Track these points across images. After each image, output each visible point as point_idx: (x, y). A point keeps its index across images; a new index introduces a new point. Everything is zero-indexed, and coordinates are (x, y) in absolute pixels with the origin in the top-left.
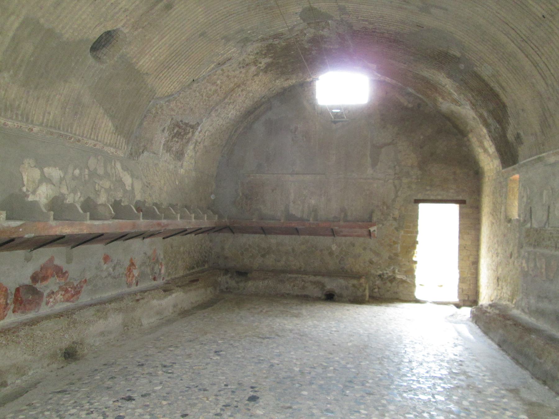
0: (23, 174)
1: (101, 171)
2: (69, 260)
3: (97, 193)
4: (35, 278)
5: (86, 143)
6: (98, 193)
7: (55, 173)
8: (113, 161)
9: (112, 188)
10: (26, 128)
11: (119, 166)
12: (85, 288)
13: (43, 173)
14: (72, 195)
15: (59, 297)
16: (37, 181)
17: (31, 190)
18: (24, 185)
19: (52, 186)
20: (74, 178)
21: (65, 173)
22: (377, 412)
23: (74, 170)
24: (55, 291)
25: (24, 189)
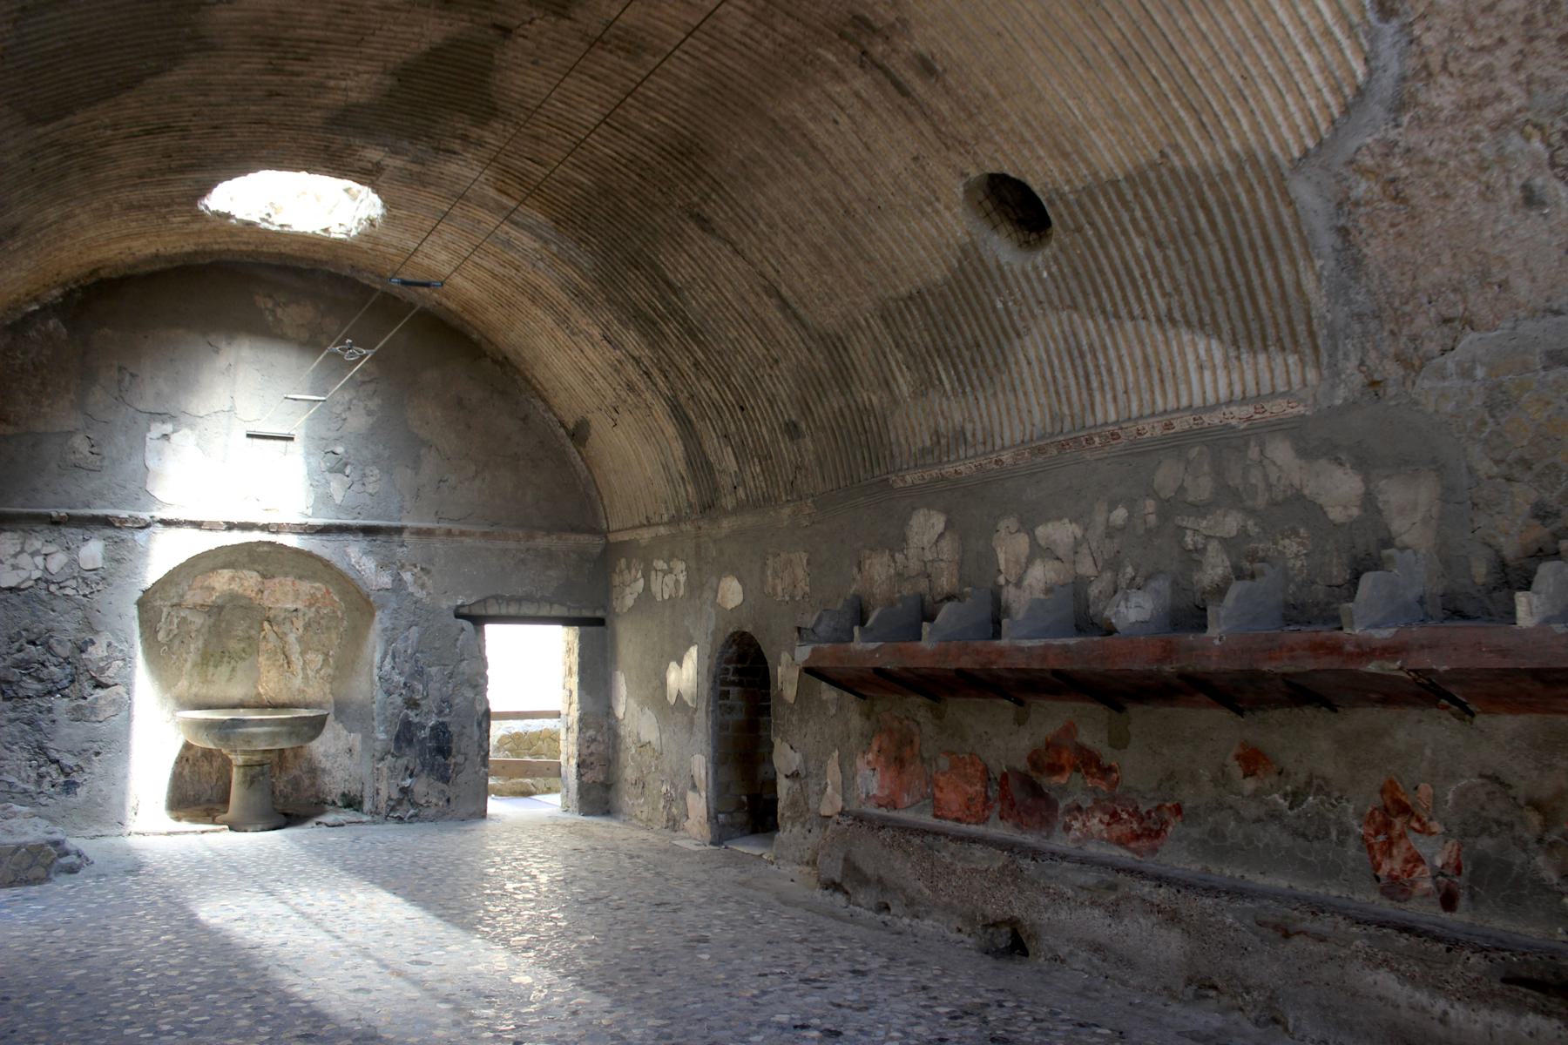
0: (999, 550)
1: (1202, 488)
2: (1119, 741)
3: (1193, 558)
5: (1140, 434)
6: (1195, 556)
7: (1060, 532)
8: (1252, 444)
9: (1253, 529)
11: (1281, 452)
12: (1174, 827)
13: (1033, 540)
14: (1108, 575)
15: (1095, 823)
16: (1023, 560)
17: (1013, 579)
18: (999, 571)
19: (1057, 564)
20: (1111, 532)
21: (1086, 529)
22: (270, 1010)
23: (1110, 511)
24: (1084, 806)
25: (1001, 580)
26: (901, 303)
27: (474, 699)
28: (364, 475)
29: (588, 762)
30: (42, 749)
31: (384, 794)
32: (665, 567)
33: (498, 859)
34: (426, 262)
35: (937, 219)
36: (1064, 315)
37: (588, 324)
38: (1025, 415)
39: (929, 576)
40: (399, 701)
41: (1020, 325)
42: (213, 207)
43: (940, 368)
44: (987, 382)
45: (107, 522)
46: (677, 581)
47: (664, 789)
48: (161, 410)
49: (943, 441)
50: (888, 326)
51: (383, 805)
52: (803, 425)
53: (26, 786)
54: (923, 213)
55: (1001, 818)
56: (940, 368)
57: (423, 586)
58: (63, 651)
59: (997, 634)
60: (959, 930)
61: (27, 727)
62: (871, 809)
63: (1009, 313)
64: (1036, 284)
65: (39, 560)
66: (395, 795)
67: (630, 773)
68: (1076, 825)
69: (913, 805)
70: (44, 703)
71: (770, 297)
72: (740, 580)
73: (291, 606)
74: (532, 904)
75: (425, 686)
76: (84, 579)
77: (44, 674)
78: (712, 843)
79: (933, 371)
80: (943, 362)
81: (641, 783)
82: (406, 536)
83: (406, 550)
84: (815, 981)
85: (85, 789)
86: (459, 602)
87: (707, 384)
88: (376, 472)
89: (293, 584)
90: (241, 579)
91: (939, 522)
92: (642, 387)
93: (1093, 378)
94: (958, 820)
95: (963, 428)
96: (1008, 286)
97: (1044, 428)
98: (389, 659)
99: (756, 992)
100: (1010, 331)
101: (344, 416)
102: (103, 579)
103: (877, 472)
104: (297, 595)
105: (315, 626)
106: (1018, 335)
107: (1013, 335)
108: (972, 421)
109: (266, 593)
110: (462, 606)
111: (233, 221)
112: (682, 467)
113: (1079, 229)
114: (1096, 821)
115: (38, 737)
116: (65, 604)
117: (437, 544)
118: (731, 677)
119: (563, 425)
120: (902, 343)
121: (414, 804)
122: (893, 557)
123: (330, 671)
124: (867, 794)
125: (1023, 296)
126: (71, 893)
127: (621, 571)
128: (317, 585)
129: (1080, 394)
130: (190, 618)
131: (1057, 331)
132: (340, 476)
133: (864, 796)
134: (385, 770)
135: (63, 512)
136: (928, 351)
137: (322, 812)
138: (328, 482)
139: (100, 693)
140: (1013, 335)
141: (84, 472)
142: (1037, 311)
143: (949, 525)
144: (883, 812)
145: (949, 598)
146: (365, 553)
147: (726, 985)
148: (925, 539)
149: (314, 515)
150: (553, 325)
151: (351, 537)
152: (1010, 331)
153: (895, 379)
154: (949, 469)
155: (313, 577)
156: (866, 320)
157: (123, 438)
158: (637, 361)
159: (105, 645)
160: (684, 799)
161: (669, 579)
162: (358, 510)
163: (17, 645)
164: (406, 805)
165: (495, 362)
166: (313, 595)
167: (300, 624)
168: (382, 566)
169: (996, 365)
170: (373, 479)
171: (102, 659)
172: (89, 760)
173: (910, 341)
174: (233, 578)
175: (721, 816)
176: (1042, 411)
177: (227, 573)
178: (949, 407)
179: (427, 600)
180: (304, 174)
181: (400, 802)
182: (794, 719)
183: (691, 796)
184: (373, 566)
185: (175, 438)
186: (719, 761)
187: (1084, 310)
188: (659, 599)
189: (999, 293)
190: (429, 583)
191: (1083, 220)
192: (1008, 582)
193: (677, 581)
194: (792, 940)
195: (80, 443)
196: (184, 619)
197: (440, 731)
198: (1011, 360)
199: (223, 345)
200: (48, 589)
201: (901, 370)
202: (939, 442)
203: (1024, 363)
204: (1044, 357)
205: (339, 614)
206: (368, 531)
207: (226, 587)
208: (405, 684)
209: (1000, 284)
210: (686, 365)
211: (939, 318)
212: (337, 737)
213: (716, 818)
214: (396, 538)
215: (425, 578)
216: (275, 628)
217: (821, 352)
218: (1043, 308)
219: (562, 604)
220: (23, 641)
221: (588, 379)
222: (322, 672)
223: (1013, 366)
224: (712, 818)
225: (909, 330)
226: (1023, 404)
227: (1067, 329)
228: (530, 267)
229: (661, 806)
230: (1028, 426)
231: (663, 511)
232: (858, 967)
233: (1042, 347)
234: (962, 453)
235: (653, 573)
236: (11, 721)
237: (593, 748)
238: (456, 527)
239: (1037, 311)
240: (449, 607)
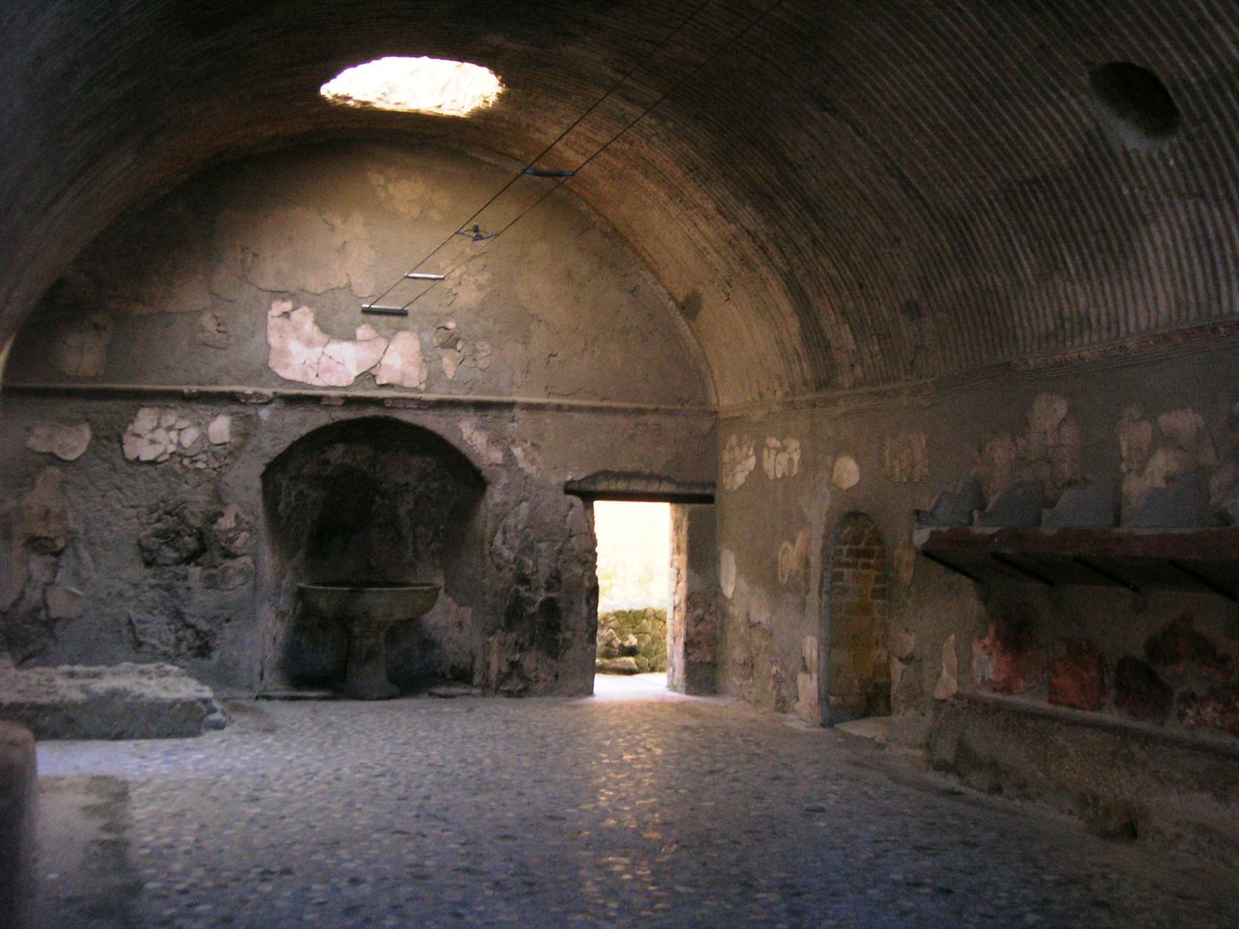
4: (1153, 649)
7: (1184, 422)
10: (1114, 348)
15: (1209, 712)
16: (1145, 447)
17: (1134, 467)
22: (431, 848)
24: (1199, 694)
25: (1123, 467)
26: (1027, 188)
27: (583, 575)
28: (475, 351)
29: (695, 641)
30: (178, 615)
31: (494, 667)
32: (778, 444)
33: (612, 733)
34: (537, 136)
35: (1063, 106)
36: (1190, 203)
37: (702, 199)
38: (1150, 301)
39: (1050, 462)
40: (509, 575)
41: (1146, 211)
42: (334, 92)
43: (1066, 253)
44: (1112, 267)
45: (233, 398)
46: (791, 460)
47: (774, 670)
48: (281, 288)
49: (1068, 326)
50: (1012, 209)
51: (493, 677)
52: (924, 304)
53: (166, 649)
54: (1049, 99)
55: (1117, 704)
56: (1066, 253)
57: (533, 462)
58: (196, 522)
59: (1117, 522)
60: (1071, 813)
61: (165, 593)
62: (986, 694)
63: (1136, 202)
64: (1163, 172)
65: (173, 435)
66: (505, 669)
67: (738, 654)
68: (1190, 712)
69: (1028, 689)
70: (180, 570)
71: (892, 175)
72: (857, 461)
74: (651, 774)
75: (535, 562)
76: (214, 453)
77: (179, 544)
78: (823, 725)
79: (1058, 254)
80: (1069, 247)
81: (749, 666)
82: (517, 412)
83: (517, 425)
84: (928, 848)
86: (569, 478)
87: (826, 262)
88: (487, 347)
91: (1061, 408)
92: (758, 262)
93: (1219, 266)
94: (1073, 706)
95: (1087, 312)
96: (1135, 174)
97: (1170, 317)
99: (872, 855)
100: (1137, 217)
101: (455, 291)
103: (1000, 355)
106: (1145, 222)
107: (1139, 222)
108: (1096, 305)
109: (378, 468)
110: (572, 482)
111: (351, 103)
112: (797, 342)
113: (1206, 118)
114: (1210, 710)
115: (176, 602)
117: (547, 419)
118: (844, 559)
119: (673, 298)
120: (1027, 226)
121: (523, 678)
122: (1014, 440)
124: (983, 679)
125: (1151, 183)
126: (223, 745)
127: (732, 448)
128: (427, 459)
129: (1206, 283)
131: (1183, 218)
132: (452, 351)
133: (979, 680)
134: (496, 644)
135: (195, 389)
136: (1053, 235)
137: (435, 685)
138: (440, 358)
139: (228, 563)
140: (1139, 222)
141: (212, 350)
142: (1164, 198)
143: (1072, 411)
144: (999, 696)
145: (1069, 484)
146: (481, 428)
147: (843, 848)
148: (1048, 424)
149: (427, 391)
150: (666, 198)
151: (463, 413)
152: (1137, 217)
153: (1020, 262)
154: (1073, 354)
156: (991, 203)
157: (246, 316)
158: (753, 236)
160: (794, 680)
161: (783, 458)
162: (469, 385)
163: (155, 516)
164: (515, 679)
165: (605, 234)
167: (410, 498)
168: (494, 441)
169: (1122, 251)
170: (483, 354)
171: (231, 530)
172: (220, 626)
173: (1034, 223)
174: (346, 453)
175: (832, 699)
176: (1167, 298)
177: (340, 448)
178: (1074, 290)
179: (537, 476)
180: (425, 59)
181: (508, 676)
182: (910, 602)
183: (802, 678)
184: (484, 441)
185: (295, 315)
186: (831, 643)
187: (1211, 198)
188: (771, 477)
189: (1125, 179)
190: (539, 458)
191: (1210, 111)
192: (1130, 470)
193: (791, 460)
194: (905, 814)
195: (207, 321)
197: (550, 607)
198: (1137, 245)
199: (337, 222)
200: (181, 462)
201: (1025, 252)
202: (1063, 325)
203: (1149, 250)
204: (1170, 243)
206: (481, 406)
207: (339, 461)
208: (515, 559)
209: (1127, 171)
210: (803, 240)
211: (1065, 203)
213: (827, 700)
214: (507, 414)
215: (536, 454)
217: (943, 231)
218: (1169, 196)
219: (669, 480)
220: (160, 512)
221: (701, 253)
222: (432, 546)
223: (1139, 252)
224: (823, 699)
225: (1035, 213)
226: (1149, 292)
227: (1194, 216)
228: (644, 141)
229: (770, 688)
230: (1153, 312)
231: (776, 386)
232: (967, 839)
233: (1168, 235)
234: (1086, 339)
235: (765, 452)
236: (152, 587)
237: (700, 627)
238: (566, 401)
239: (1164, 198)
240: (559, 484)
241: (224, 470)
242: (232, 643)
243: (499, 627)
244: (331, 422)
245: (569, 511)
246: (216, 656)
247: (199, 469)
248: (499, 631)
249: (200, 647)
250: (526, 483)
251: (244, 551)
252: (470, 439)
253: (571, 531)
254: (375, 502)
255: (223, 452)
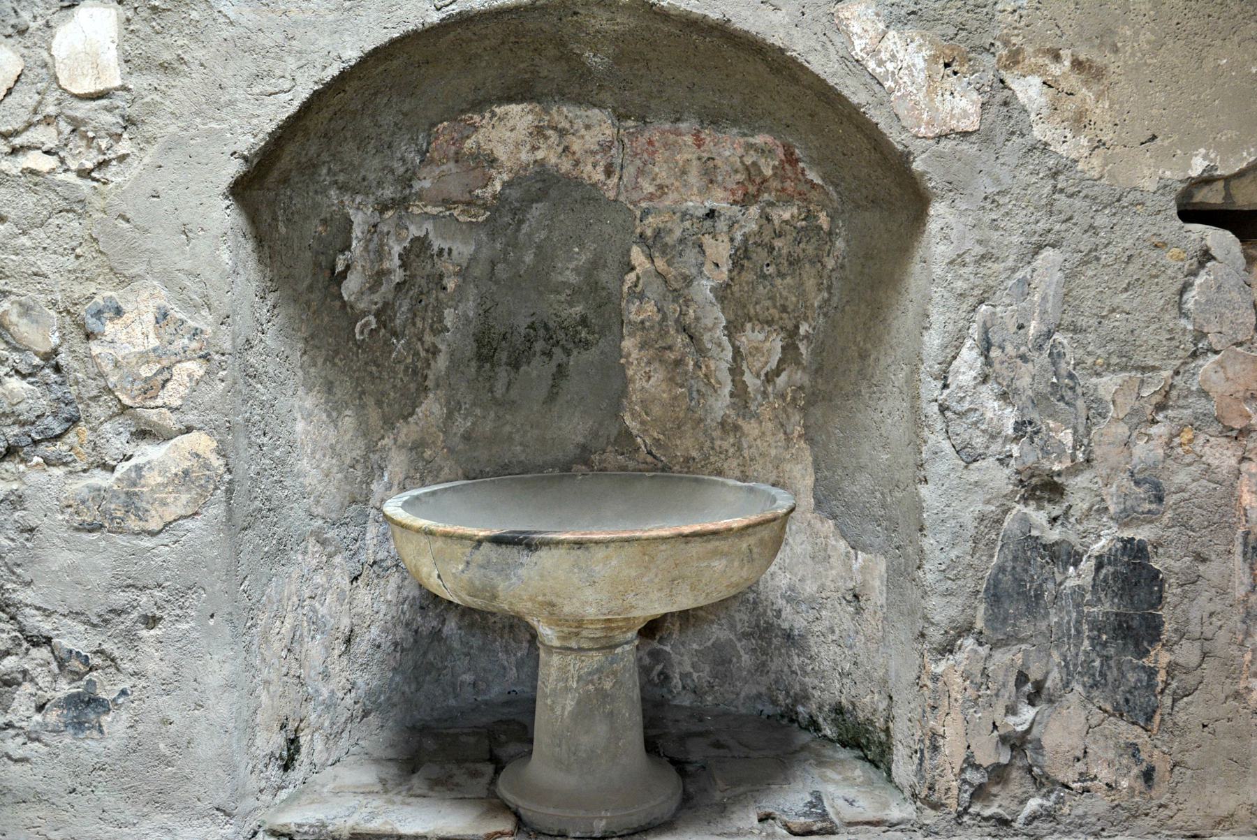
31: (952, 750)
40: (1001, 479)
57: (1079, 121)
73: (696, 204)
76: (76, 126)
85: (124, 716)
86: (1197, 167)
89: (699, 143)
90: (562, 133)
98: (969, 355)
102: (129, 122)
104: (710, 176)
105: (761, 255)
110: (1206, 180)
116: (30, 200)
121: (1042, 782)
123: (800, 377)
128: (760, 139)
130: (437, 244)
139: (150, 452)
155: (747, 120)
159: (150, 318)
166: (751, 171)
167: (719, 249)
171: (144, 357)
172: (130, 638)
174: (539, 132)
177: (519, 115)
179: (1093, 166)
190: (1099, 111)
196: (421, 244)
205: (823, 220)
207: (524, 156)
208: (1020, 426)
212: (821, 556)
215: (1086, 94)
216: (660, 264)
222: (781, 380)
241: (109, 173)
242: (168, 686)
243: (966, 629)
244: (435, 18)
245: (1194, 274)
246: (115, 724)
247: (33, 172)
248: (969, 643)
249: (73, 701)
250: (1055, 190)
251: (191, 418)
252: (875, 52)
253: (1201, 335)
254: (633, 269)
255: (108, 119)
